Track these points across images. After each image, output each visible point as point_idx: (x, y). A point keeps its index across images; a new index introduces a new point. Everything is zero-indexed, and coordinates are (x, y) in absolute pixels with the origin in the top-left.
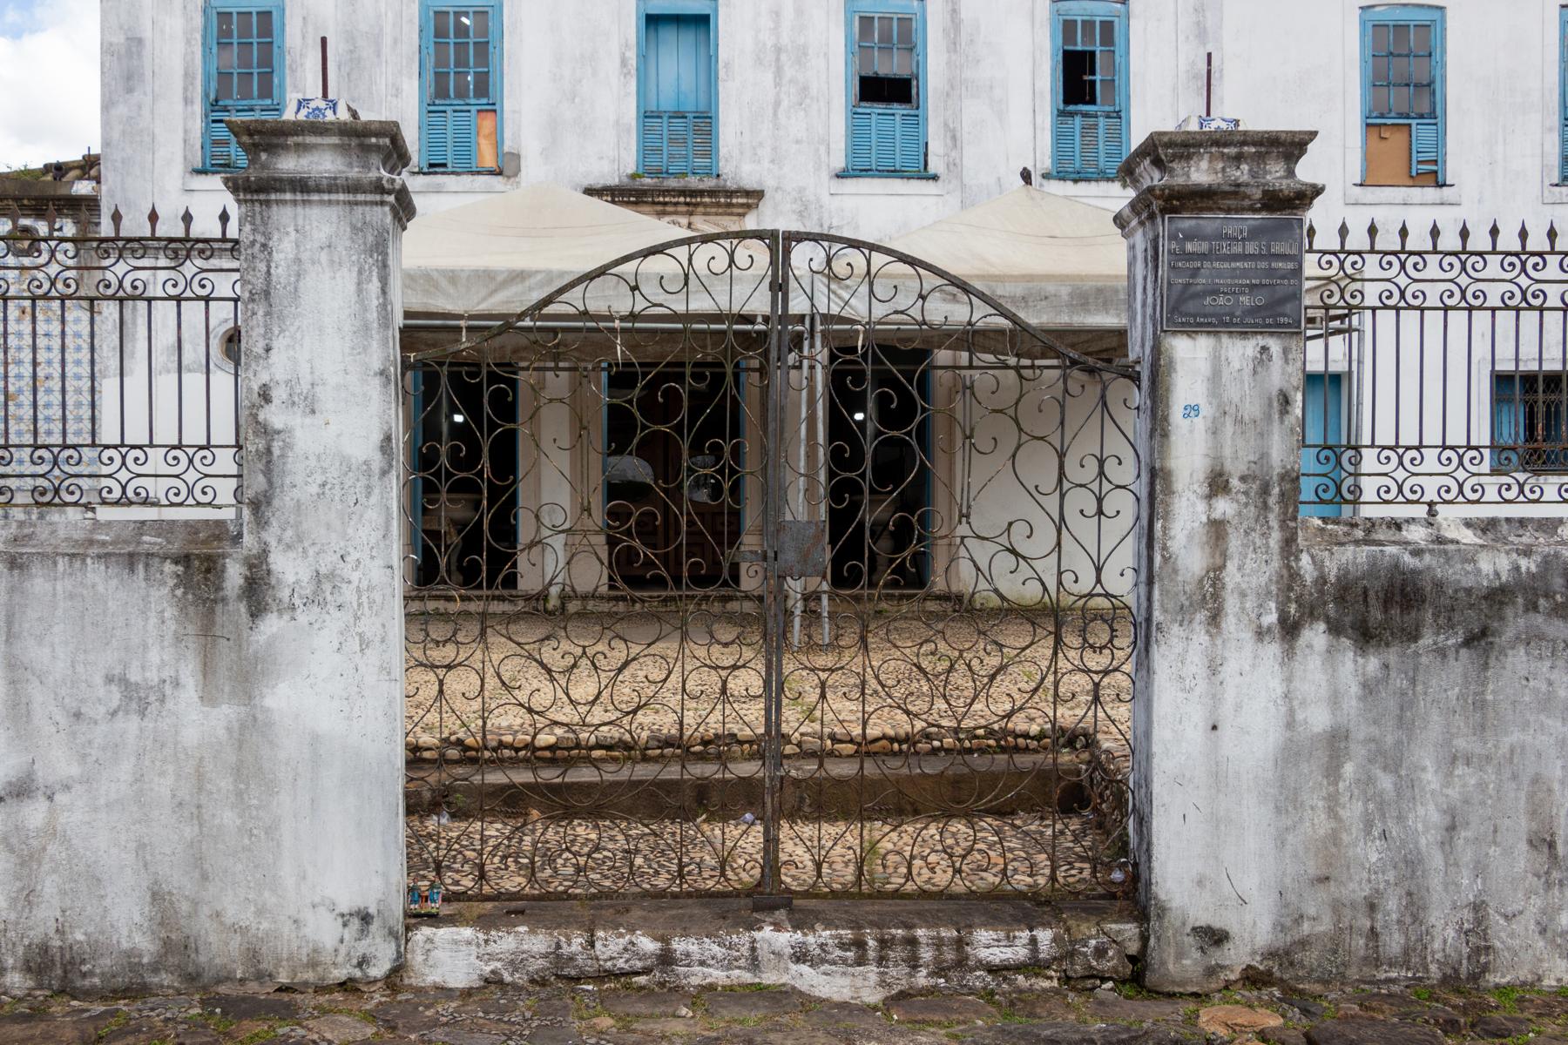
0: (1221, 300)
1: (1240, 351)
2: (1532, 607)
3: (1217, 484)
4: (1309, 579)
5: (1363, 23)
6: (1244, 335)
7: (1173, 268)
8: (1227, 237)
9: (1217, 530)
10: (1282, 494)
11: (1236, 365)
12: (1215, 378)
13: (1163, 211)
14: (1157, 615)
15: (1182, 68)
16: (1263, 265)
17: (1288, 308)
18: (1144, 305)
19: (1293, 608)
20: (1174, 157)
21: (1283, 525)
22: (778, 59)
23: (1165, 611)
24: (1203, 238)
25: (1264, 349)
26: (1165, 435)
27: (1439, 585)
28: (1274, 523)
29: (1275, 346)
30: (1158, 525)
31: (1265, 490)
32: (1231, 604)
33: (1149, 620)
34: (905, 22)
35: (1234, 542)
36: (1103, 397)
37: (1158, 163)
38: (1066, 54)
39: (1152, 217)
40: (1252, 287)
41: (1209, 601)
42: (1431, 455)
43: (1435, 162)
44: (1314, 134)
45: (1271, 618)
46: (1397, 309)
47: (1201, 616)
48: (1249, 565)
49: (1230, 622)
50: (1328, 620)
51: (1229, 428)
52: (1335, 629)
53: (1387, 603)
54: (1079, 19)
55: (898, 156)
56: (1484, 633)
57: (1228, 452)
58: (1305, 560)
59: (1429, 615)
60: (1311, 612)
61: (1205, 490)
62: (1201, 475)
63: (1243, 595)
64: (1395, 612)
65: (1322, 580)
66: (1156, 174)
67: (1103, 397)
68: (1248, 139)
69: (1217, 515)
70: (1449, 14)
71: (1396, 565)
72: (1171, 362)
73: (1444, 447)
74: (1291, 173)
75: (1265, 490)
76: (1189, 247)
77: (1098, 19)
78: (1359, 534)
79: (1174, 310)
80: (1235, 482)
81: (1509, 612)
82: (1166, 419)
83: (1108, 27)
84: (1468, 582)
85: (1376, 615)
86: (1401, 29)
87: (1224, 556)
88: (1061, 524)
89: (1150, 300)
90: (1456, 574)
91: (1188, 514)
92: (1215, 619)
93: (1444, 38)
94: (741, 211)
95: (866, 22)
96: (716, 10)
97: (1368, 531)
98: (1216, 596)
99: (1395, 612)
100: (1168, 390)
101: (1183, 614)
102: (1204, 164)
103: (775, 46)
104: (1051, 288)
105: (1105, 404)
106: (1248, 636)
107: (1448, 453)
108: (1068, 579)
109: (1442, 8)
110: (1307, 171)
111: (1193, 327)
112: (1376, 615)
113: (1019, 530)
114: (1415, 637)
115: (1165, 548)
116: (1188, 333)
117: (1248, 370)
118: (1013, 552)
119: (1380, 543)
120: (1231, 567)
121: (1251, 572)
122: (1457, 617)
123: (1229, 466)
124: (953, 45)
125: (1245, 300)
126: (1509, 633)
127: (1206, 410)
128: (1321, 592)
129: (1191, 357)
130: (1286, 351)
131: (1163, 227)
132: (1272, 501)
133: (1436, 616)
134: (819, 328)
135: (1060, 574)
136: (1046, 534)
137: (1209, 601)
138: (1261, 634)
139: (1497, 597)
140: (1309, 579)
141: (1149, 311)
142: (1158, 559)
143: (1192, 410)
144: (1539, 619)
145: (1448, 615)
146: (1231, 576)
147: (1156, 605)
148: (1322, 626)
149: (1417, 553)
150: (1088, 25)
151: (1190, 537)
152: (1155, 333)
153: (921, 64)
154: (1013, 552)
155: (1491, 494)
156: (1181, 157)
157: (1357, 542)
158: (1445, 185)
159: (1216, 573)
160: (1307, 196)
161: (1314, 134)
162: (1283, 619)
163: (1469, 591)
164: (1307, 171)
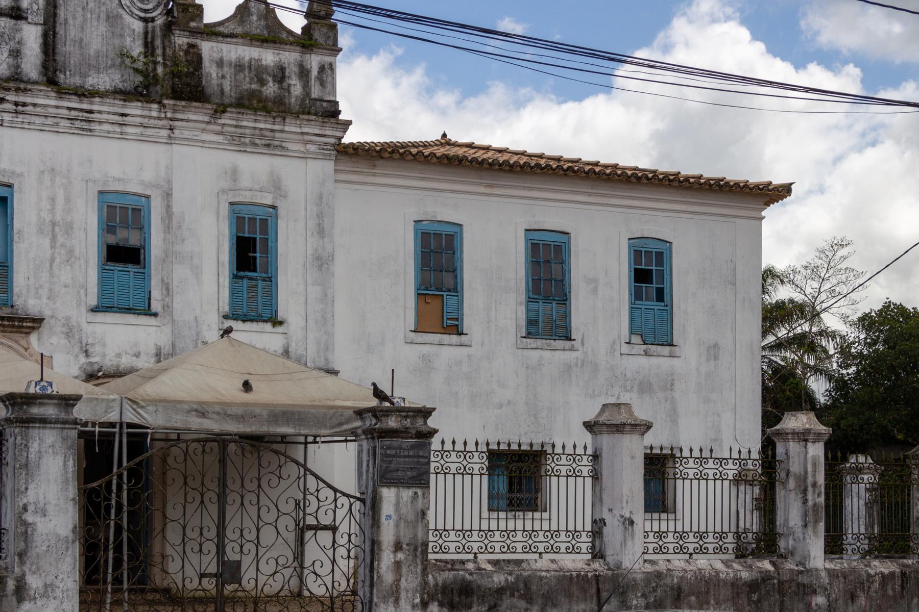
0: (400, 473)
1: (407, 494)
2: (513, 595)
3: (398, 547)
4: (431, 585)
5: (416, 231)
6: (408, 487)
7: (382, 460)
8: (402, 449)
9: (398, 565)
10: (422, 551)
11: (405, 499)
12: (397, 504)
13: (379, 437)
14: (375, 599)
15: (309, 252)
16: (415, 460)
17: (425, 477)
18: (367, 471)
19: (426, 596)
20: (382, 415)
21: (422, 564)
22: (53, 231)
23: (378, 598)
24: (393, 449)
25: (416, 493)
26: (379, 527)
27: (479, 587)
28: (419, 563)
29: (420, 492)
30: (376, 563)
31: (416, 549)
32: (403, 595)
33: (371, 601)
34: (137, 211)
35: (404, 570)
36: (350, 509)
37: (375, 416)
38: (238, 238)
39: (373, 438)
40: (411, 468)
41: (394, 594)
42: (475, 533)
43: (457, 319)
44: (435, 409)
45: (418, 600)
46: (463, 474)
47: (391, 600)
48: (410, 579)
49: (402, 602)
50: (439, 601)
51: (402, 525)
52: (441, 605)
53: (460, 595)
54: (247, 216)
55: (131, 298)
56: (495, 606)
57: (402, 534)
58: (430, 577)
59: (475, 599)
60: (432, 598)
61: (393, 549)
62: (392, 543)
63: (407, 591)
64: (463, 597)
65: (436, 585)
66: (374, 421)
67: (350, 509)
68: (410, 410)
69: (398, 559)
70: (465, 229)
71: (463, 579)
72: (381, 499)
73: (480, 531)
74: (426, 423)
75: (416, 549)
76: (388, 452)
77: (258, 217)
78: (449, 566)
79: (382, 477)
80: (404, 546)
81: (504, 597)
82: (379, 520)
83: (264, 222)
84: (489, 585)
85: (456, 599)
86: (438, 235)
87: (401, 576)
88: (334, 562)
89: (371, 470)
90: (485, 582)
91: (387, 559)
92: (397, 601)
93: (462, 244)
94: (27, 330)
95: (111, 208)
96: (12, 195)
97: (452, 565)
98: (398, 592)
99: (463, 597)
100: (380, 509)
101: (385, 599)
102: (393, 419)
103: (51, 221)
104: (258, 411)
105: (351, 512)
106: (409, 607)
107: (482, 533)
108: (336, 584)
109: (460, 225)
110: (432, 423)
111: (390, 483)
112: (456, 599)
113: (318, 564)
114: (470, 608)
115: (378, 572)
116: (388, 487)
117: (410, 501)
118: (315, 573)
119: (457, 570)
120: (403, 580)
121: (410, 582)
122: (485, 599)
123: (402, 540)
124: (168, 228)
125: (409, 474)
126: (504, 606)
127: (394, 517)
128: (436, 590)
129: (388, 495)
130: (424, 494)
131: (378, 443)
132: (418, 553)
133: (478, 599)
134: (125, 430)
135: (333, 582)
136: (328, 565)
137: (394, 594)
138: (414, 606)
139: (500, 591)
140: (431, 585)
141: (371, 475)
142: (375, 577)
143: (389, 517)
144: (515, 600)
145: (482, 598)
146: (403, 584)
147: (375, 595)
148: (436, 604)
149: (471, 574)
150: (252, 220)
151: (388, 568)
152: (374, 485)
153: (146, 239)
154: (315, 573)
155: (497, 550)
156: (385, 416)
157: (449, 570)
158: (462, 334)
159: (397, 581)
160: (432, 433)
161: (435, 409)
162: (422, 601)
163: (490, 589)
164: (432, 423)
